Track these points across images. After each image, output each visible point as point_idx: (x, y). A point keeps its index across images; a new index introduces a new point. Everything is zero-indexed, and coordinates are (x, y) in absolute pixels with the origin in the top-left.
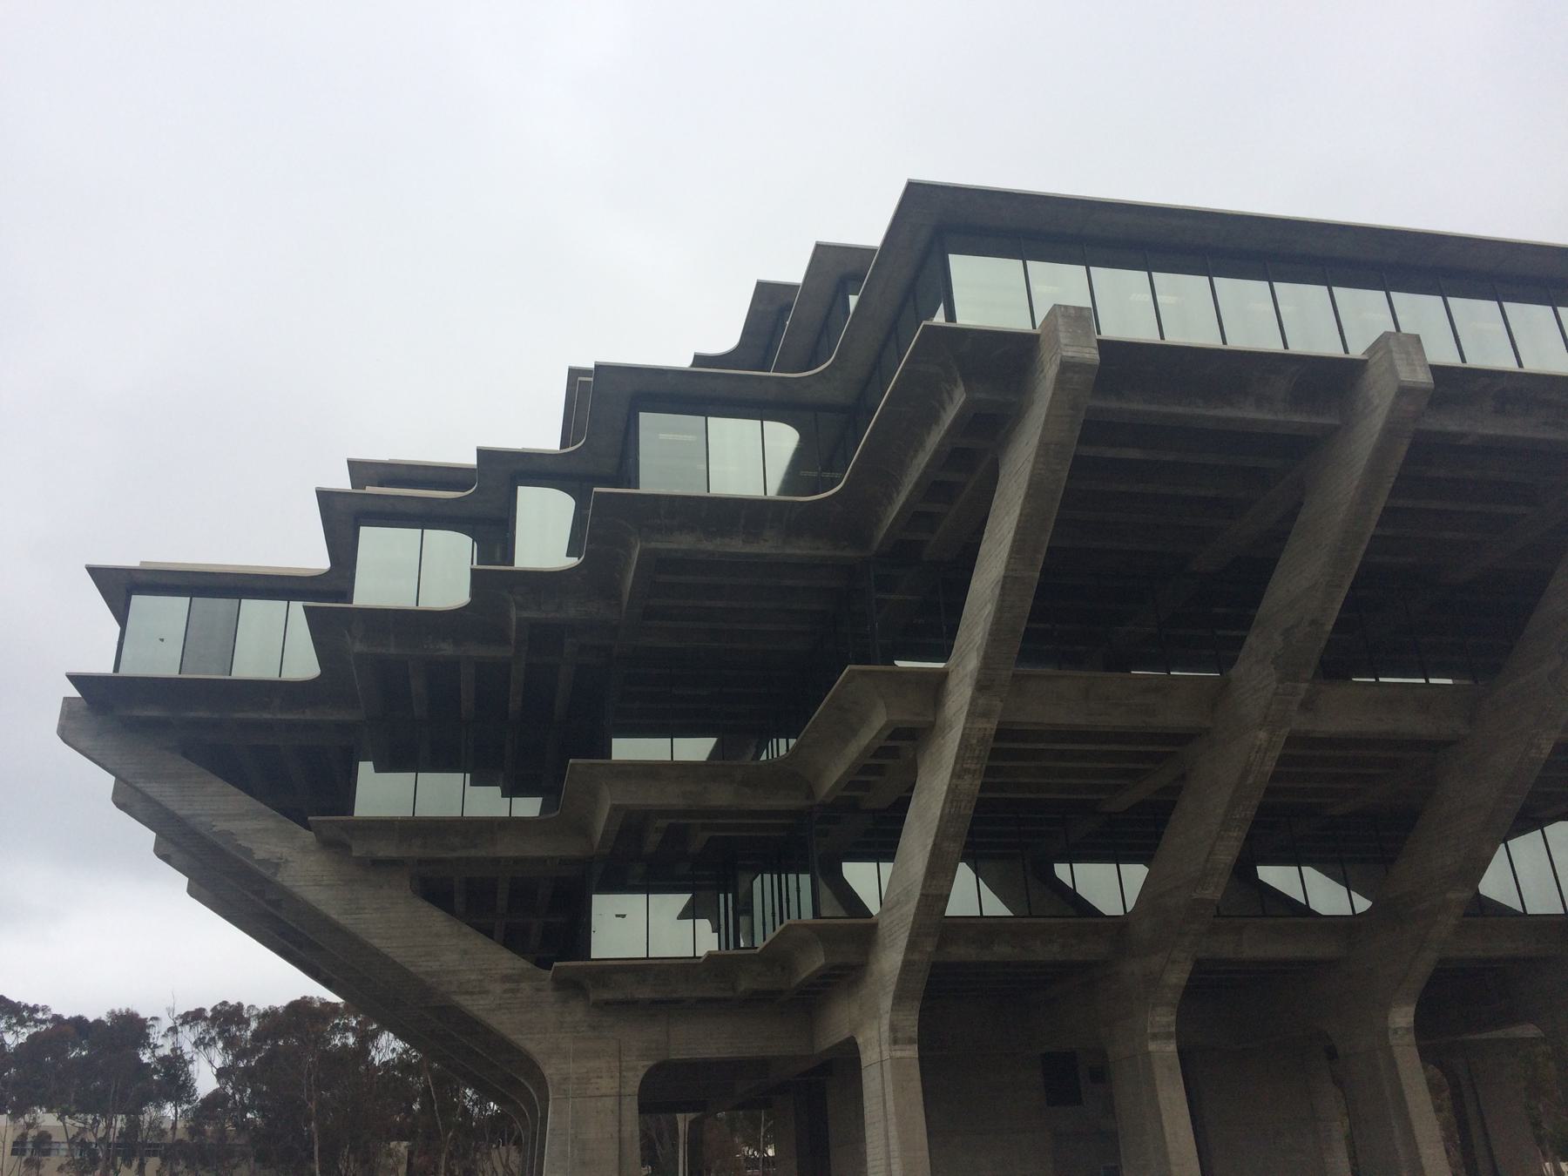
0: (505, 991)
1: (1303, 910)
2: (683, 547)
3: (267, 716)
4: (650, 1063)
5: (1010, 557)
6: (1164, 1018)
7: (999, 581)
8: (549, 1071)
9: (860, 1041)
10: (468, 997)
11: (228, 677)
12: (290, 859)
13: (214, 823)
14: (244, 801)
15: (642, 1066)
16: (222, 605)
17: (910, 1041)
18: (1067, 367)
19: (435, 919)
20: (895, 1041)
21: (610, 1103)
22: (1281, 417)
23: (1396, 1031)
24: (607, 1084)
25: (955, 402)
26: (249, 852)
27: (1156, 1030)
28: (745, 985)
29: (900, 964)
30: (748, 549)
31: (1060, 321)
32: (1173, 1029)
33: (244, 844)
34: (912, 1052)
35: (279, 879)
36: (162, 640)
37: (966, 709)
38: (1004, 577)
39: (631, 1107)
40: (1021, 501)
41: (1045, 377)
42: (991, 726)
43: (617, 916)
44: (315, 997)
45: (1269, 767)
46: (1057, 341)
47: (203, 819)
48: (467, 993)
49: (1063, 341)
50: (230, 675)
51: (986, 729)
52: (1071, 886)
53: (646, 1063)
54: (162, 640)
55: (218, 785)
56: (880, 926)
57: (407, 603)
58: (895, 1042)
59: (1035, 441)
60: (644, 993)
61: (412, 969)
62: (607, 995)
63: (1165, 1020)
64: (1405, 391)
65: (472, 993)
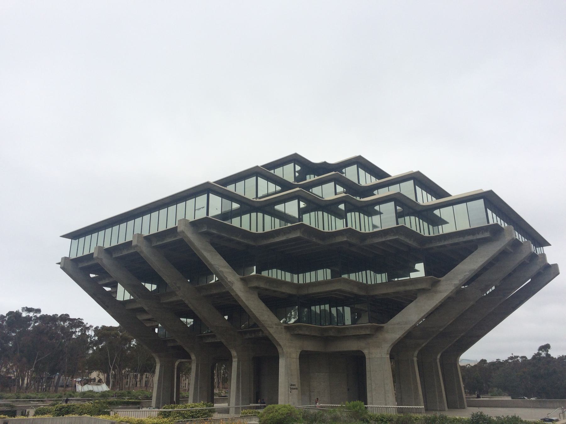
0: (276, 328)
4: (301, 351)
6: (416, 353)
9: (366, 352)
12: (235, 282)
13: (219, 268)
15: (300, 351)
19: (263, 305)
20: (387, 354)
26: (226, 278)
34: (388, 356)
48: (269, 327)
53: (300, 350)
55: (219, 256)
58: (387, 354)
60: (307, 333)
61: (259, 319)
62: (301, 332)
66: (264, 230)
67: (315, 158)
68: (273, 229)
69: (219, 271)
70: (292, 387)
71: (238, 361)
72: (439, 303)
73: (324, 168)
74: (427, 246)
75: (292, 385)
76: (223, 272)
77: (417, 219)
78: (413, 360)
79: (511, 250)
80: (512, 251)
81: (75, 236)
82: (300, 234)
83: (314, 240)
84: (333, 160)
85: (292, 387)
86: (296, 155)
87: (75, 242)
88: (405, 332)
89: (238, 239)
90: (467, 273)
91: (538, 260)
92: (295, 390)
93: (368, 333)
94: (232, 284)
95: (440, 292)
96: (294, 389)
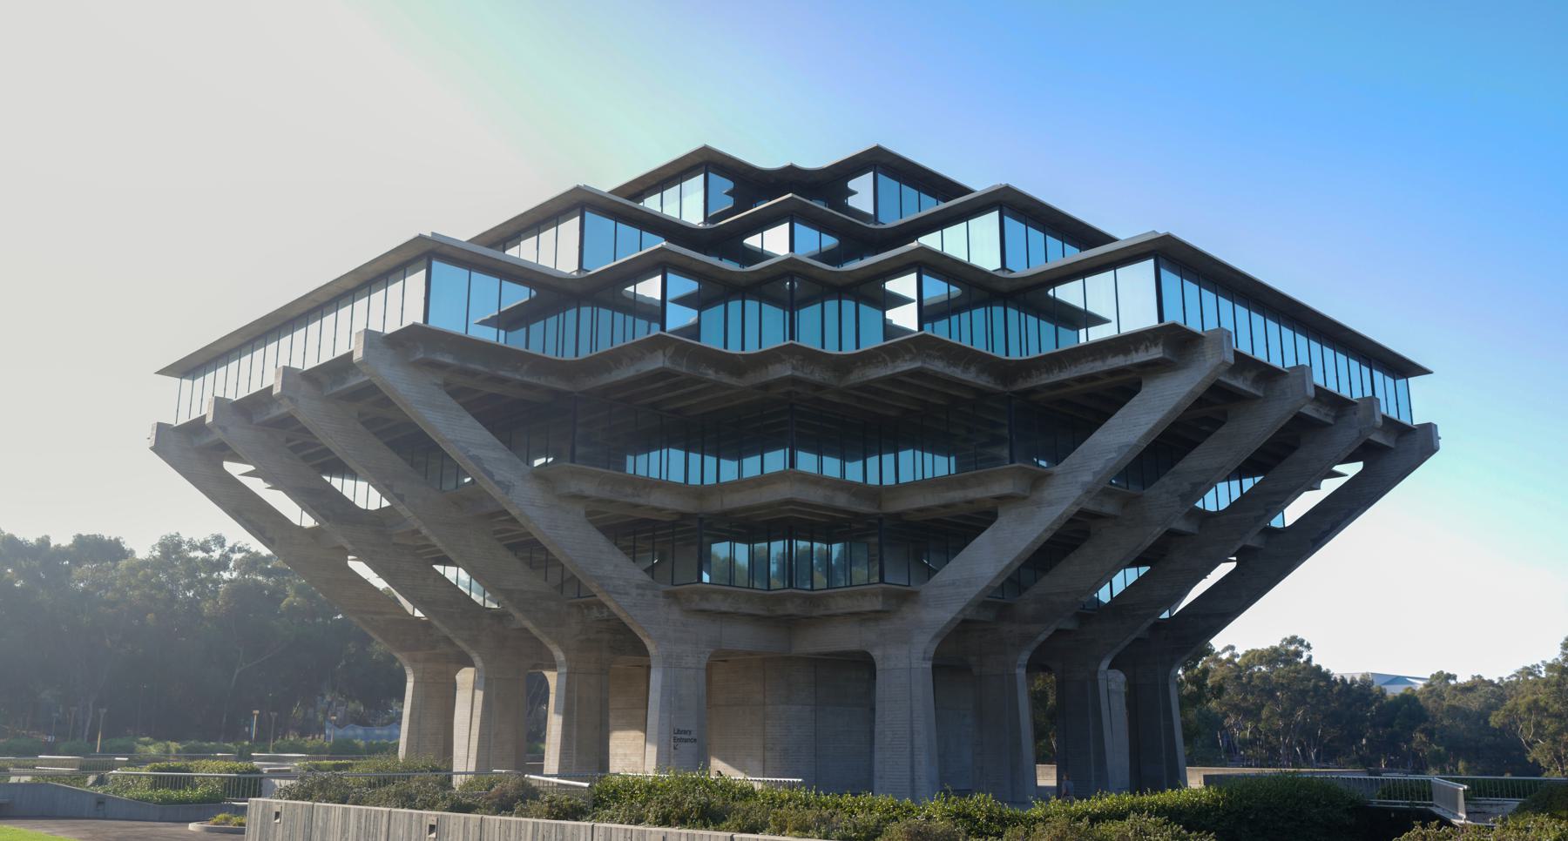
2: (938, 370)
9: (876, 654)
13: (469, 448)
17: (929, 660)
20: (924, 659)
25: (1149, 353)
29: (949, 618)
34: (929, 665)
40: (1166, 412)
49: (1225, 349)
53: (709, 650)
55: (469, 420)
58: (924, 659)
60: (725, 607)
62: (706, 606)
65: (620, 594)
66: (577, 355)
67: (766, 156)
68: (594, 353)
70: (679, 736)
71: (567, 673)
72: (1046, 531)
73: (790, 178)
74: (1022, 385)
75: (679, 732)
77: (1023, 315)
78: (1015, 674)
79: (1252, 390)
80: (1260, 394)
81: (191, 367)
83: (711, 374)
84: (816, 157)
86: (705, 150)
87: (187, 383)
88: (964, 604)
89: (518, 377)
90: (1114, 455)
91: (1355, 414)
93: (879, 607)
95: (1050, 504)
96: (686, 741)
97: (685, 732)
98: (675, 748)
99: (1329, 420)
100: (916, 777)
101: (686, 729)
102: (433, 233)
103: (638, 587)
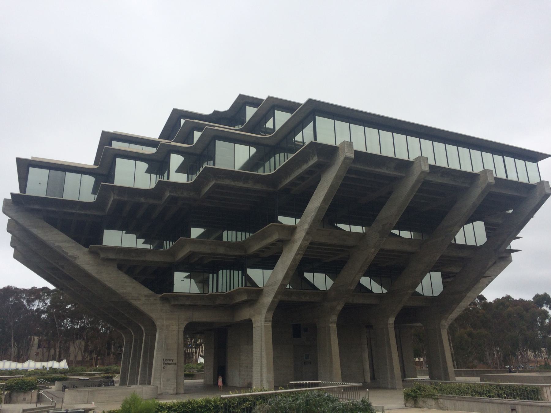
0: (146, 300)
1: (370, 291)
2: (227, 184)
3: (74, 211)
4: (188, 322)
5: (322, 202)
6: (334, 318)
7: (317, 208)
8: (158, 323)
9: (253, 320)
10: (134, 301)
11: (61, 198)
12: (80, 256)
14: (65, 237)
15: (185, 323)
16: (60, 173)
17: (270, 321)
18: (346, 158)
20: (266, 321)
21: (175, 333)
22: (392, 173)
23: (390, 324)
24: (175, 328)
26: (66, 253)
27: (332, 321)
28: (218, 302)
29: (271, 301)
30: (244, 186)
31: (346, 145)
32: (336, 321)
33: (66, 251)
35: (76, 262)
36: (40, 184)
37: (302, 238)
38: (320, 207)
39: (182, 334)
40: (328, 188)
41: (339, 159)
42: (307, 243)
43: (181, 280)
44: (13, 286)
45: (373, 257)
46: (345, 151)
47: (51, 242)
48: (134, 300)
49: (346, 151)
50: (63, 198)
51: (306, 244)
52: (313, 283)
53: (186, 322)
54: (40, 184)
55: (56, 231)
56: (264, 290)
57: (131, 185)
59: (334, 175)
60: (188, 303)
62: (177, 303)
63: (334, 318)
64: (423, 172)
65: (136, 300)
69: (55, 246)
70: (166, 362)
72: (296, 255)
73: (217, 117)
75: (166, 360)
76: (61, 247)
78: (329, 327)
80: (404, 175)
82: (114, 196)
84: (225, 105)
85: (166, 362)
91: (479, 180)
92: (172, 366)
94: (76, 258)
96: (170, 364)
97: (170, 360)
98: (163, 368)
99: (467, 185)
100: (263, 379)
101: (171, 359)
102: (32, 157)
103: (146, 296)
